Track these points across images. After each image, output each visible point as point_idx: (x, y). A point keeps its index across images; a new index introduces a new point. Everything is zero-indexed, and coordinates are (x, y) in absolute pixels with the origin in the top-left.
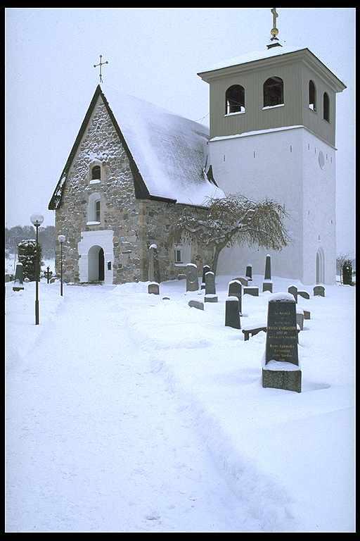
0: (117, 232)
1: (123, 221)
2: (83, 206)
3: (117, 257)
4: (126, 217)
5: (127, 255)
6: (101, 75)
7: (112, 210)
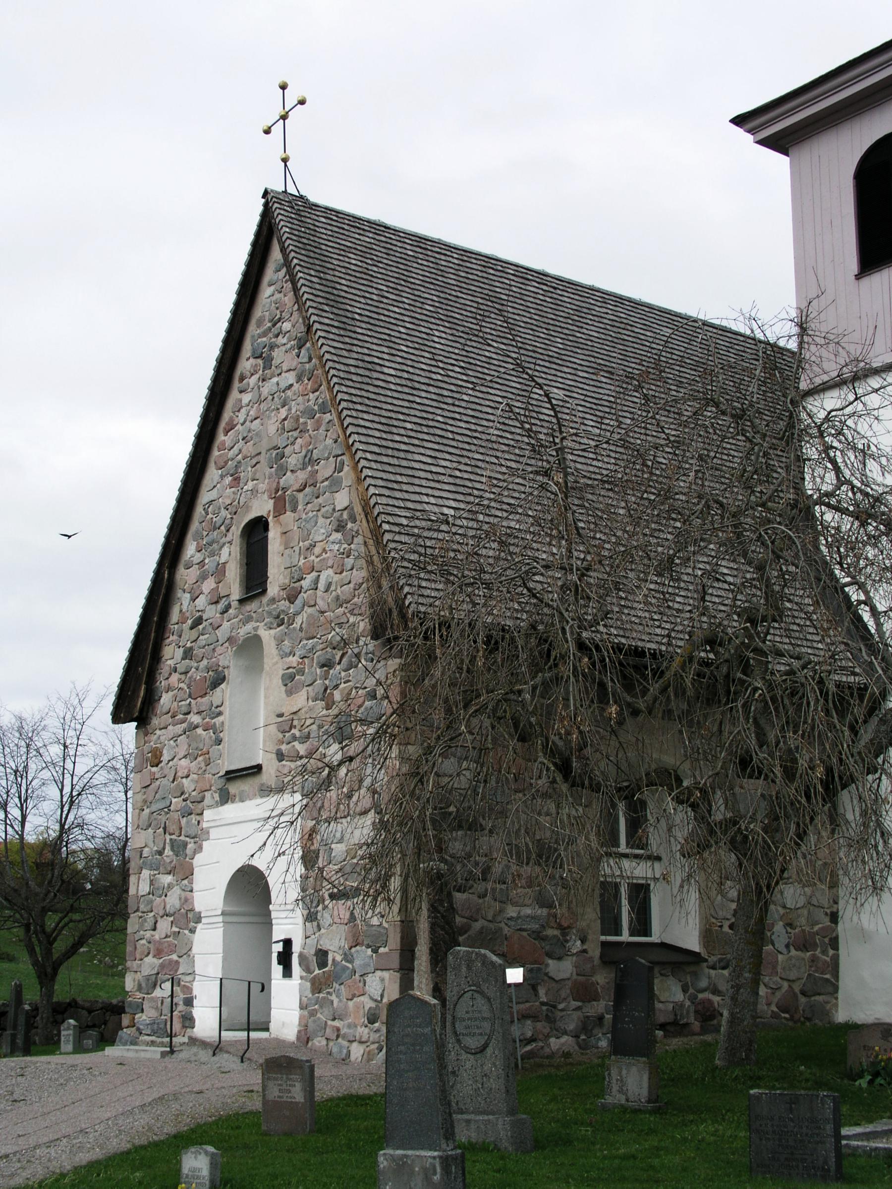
2: (216, 696)
3: (311, 917)
6: (285, 160)
7: (300, 700)
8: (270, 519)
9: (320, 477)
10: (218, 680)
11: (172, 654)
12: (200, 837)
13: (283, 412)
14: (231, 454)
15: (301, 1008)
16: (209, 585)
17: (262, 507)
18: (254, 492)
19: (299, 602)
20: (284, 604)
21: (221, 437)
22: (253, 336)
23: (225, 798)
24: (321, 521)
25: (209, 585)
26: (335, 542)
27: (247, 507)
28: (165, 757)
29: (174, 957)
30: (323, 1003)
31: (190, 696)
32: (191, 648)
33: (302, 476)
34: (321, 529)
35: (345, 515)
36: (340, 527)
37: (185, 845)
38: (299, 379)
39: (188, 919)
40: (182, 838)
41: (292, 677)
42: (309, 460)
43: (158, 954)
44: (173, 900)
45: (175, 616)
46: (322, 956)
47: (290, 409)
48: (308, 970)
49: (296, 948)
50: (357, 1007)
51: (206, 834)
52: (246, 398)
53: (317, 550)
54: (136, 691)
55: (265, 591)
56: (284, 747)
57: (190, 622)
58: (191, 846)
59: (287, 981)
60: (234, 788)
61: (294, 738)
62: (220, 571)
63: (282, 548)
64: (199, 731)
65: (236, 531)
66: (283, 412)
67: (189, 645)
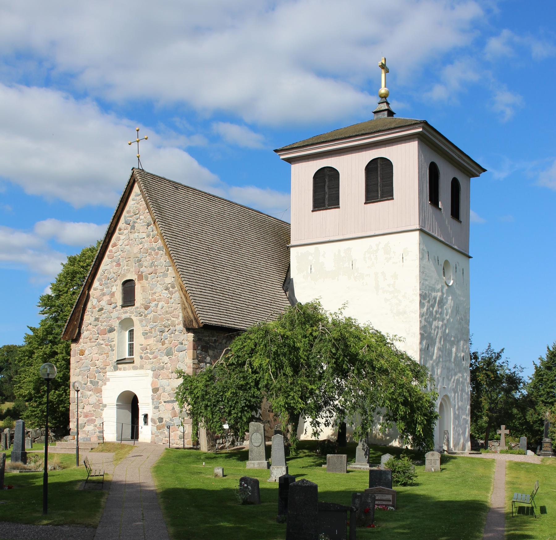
0: (157, 372)
1: (166, 359)
3: (156, 408)
4: (169, 353)
5: (170, 406)
7: (151, 341)
8: (136, 281)
9: (158, 271)
10: (111, 330)
11: (88, 318)
12: (105, 381)
13: (141, 246)
14: (115, 255)
15: (152, 434)
16: (106, 298)
17: (133, 277)
18: (128, 270)
19: (149, 310)
20: (143, 310)
21: (110, 248)
22: (125, 216)
23: (116, 369)
24: (158, 285)
25: (106, 298)
26: (165, 294)
27: (124, 275)
28: (87, 352)
29: (94, 418)
30: (161, 433)
31: (98, 334)
32: (98, 318)
33: (150, 270)
34: (159, 288)
35: (169, 285)
36: (167, 289)
37: (98, 382)
38: (148, 236)
39: (100, 406)
40: (96, 380)
41: (147, 334)
42: (152, 265)
43: (86, 416)
44: (93, 399)
45: (89, 305)
46: (161, 420)
47: (144, 246)
48: (155, 423)
49: (150, 417)
50: (175, 435)
51: (108, 380)
52: (122, 237)
53: (157, 295)
54: (73, 330)
55: (134, 305)
56: (143, 355)
57: (97, 309)
58: (100, 382)
59: (146, 426)
60: (119, 366)
61: (148, 353)
62: (113, 295)
63: (142, 292)
64: (103, 346)
65: (120, 283)
66: (141, 246)
67: (97, 316)
